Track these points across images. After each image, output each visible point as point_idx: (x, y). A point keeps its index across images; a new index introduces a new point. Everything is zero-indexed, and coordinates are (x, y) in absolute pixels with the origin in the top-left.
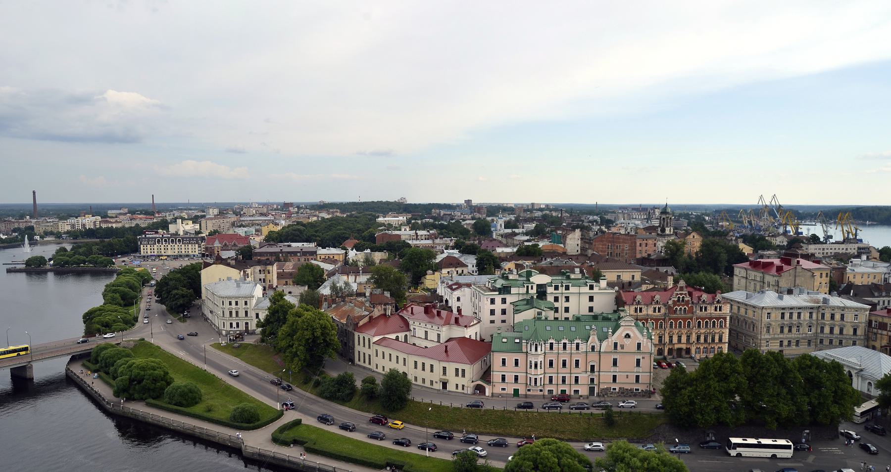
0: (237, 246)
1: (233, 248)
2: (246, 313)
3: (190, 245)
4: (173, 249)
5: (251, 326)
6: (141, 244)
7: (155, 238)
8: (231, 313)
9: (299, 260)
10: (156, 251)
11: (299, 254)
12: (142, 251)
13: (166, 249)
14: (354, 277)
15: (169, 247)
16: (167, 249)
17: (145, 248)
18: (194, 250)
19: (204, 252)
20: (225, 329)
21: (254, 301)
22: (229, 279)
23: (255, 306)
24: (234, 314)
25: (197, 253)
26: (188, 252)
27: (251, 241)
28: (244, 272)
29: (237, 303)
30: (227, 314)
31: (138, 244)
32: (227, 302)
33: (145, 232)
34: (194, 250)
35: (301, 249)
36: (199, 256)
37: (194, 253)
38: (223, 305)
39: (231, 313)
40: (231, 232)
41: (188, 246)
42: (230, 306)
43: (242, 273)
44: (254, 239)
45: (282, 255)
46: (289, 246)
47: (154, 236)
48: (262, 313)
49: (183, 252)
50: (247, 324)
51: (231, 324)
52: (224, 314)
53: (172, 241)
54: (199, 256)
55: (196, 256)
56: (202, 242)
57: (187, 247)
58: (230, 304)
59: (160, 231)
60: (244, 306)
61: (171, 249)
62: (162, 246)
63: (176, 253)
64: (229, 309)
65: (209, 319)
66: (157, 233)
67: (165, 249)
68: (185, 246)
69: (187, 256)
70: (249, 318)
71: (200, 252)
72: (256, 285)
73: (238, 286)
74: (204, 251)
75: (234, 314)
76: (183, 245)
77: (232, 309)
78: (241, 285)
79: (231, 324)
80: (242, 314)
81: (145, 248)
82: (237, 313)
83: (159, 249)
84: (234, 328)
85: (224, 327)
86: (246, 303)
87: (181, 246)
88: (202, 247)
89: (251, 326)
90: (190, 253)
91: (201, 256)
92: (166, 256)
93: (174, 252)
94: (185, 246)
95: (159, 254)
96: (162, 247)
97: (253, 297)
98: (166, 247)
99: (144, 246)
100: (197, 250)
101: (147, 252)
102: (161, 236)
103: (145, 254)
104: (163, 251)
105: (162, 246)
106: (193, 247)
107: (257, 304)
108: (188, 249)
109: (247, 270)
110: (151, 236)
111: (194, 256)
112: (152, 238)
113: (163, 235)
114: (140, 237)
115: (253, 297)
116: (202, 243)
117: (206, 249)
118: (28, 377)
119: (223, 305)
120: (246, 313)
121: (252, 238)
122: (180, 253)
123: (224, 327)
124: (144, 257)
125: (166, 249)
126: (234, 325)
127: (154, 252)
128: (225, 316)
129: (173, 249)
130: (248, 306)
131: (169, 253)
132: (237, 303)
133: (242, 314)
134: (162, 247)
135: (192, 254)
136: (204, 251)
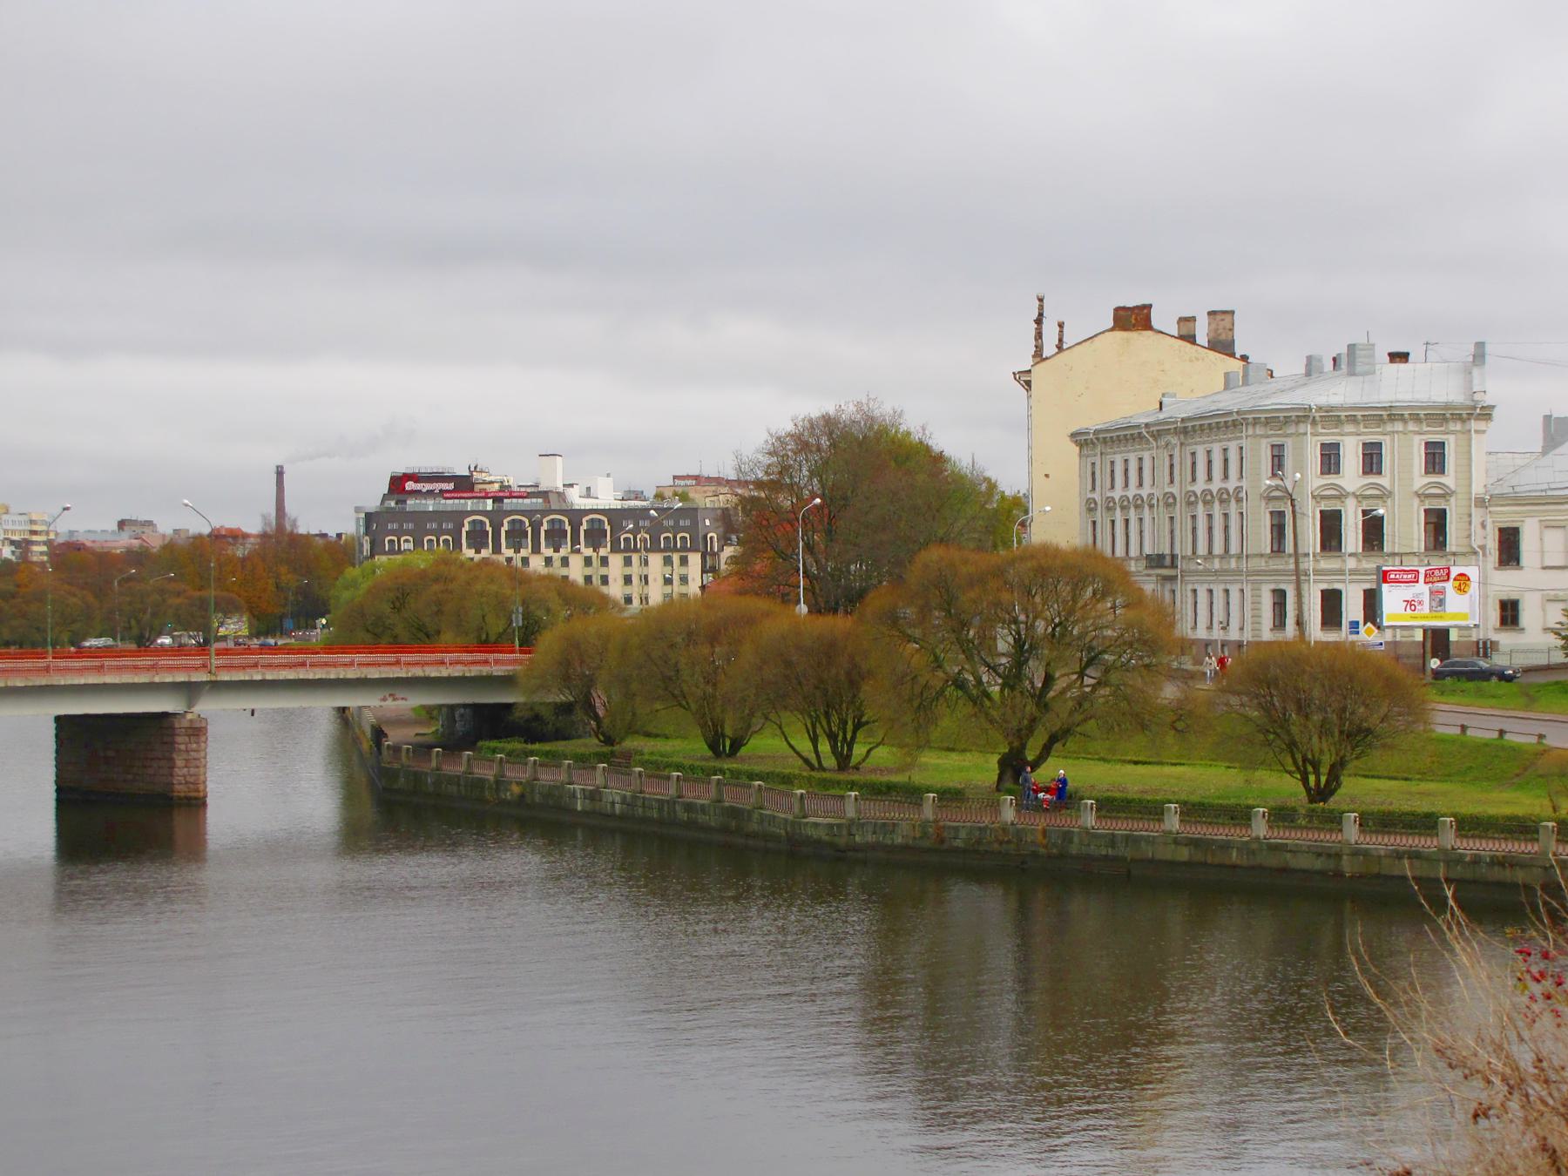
2: (1437, 524)
3: (656, 560)
8: (1331, 526)
24: (1352, 536)
29: (1372, 459)
39: (1331, 526)
51: (1332, 601)
57: (635, 570)
58: (1330, 459)
60: (1420, 480)
68: (628, 562)
75: (1352, 536)
76: (616, 561)
77: (1342, 496)
79: (1332, 601)
80: (1404, 530)
84: (1354, 625)
86: (1435, 458)
87: (604, 561)
94: (628, 562)
108: (645, 579)
110: (430, 505)
112: (438, 515)
118: (180, 789)
120: (1437, 524)
126: (1353, 608)
130: (1449, 480)
132: (1372, 459)
133: (1404, 530)
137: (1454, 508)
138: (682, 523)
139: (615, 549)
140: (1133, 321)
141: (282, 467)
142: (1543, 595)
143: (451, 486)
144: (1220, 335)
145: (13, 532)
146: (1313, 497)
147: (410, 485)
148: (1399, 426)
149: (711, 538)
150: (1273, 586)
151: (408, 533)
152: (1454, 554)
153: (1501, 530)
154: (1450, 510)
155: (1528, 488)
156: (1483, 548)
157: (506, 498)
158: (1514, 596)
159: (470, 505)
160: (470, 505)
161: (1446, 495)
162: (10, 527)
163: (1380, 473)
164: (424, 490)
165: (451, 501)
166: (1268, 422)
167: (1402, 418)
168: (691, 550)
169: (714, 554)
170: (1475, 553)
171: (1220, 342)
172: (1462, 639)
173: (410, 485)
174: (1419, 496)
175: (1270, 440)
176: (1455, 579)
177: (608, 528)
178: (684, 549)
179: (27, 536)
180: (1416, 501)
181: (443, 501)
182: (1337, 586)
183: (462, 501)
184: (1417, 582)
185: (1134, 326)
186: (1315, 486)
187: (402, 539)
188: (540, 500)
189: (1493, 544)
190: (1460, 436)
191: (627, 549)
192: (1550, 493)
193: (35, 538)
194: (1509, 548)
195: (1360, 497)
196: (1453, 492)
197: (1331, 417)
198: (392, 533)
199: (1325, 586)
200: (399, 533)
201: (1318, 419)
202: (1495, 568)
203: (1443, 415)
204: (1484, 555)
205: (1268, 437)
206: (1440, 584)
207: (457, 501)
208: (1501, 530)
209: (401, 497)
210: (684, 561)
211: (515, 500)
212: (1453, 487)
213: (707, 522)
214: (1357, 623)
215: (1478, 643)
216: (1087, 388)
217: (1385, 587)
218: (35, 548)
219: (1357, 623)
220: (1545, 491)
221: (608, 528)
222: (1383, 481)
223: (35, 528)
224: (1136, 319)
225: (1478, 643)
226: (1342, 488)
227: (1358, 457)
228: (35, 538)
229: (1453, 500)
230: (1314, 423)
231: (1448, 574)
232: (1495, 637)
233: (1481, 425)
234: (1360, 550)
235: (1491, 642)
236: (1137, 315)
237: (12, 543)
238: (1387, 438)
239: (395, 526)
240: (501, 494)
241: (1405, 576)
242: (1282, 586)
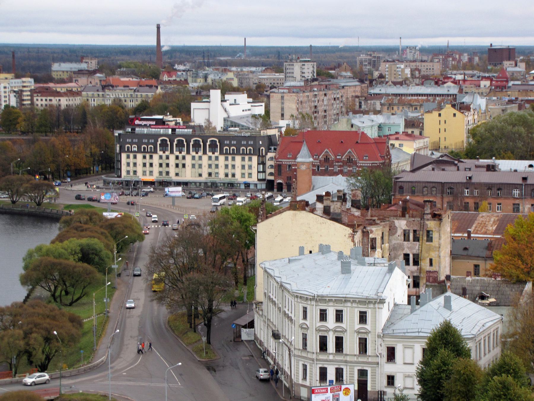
0: (355, 163)
1: (346, 169)
3: (238, 158)
4: (197, 166)
5: (374, 381)
6: (122, 150)
7: (156, 136)
9: (516, 209)
10: (156, 169)
11: (516, 192)
12: (124, 168)
13: (180, 166)
14: (247, 45)
15: (188, 160)
16: (184, 166)
17: (131, 160)
18: (246, 171)
19: (272, 178)
20: (307, 383)
21: (384, 314)
22: (324, 249)
23: (386, 327)
25: (254, 179)
26: (233, 175)
27: (392, 152)
28: (365, 234)
30: (314, 344)
31: (114, 149)
32: (314, 313)
33: (133, 120)
34: (246, 171)
35: (525, 179)
36: (259, 187)
37: (247, 180)
38: (305, 317)
40: (342, 126)
41: (233, 159)
42: (323, 323)
43: (358, 236)
44: (401, 145)
45: (472, 193)
46: (491, 168)
47: (153, 130)
48: (405, 347)
49: (222, 176)
50: (363, 373)
52: (305, 344)
53: (197, 146)
54: (259, 187)
55: (252, 187)
56: (268, 150)
58: (323, 316)
59: (169, 118)
60: (357, 326)
61: (193, 166)
62: (172, 157)
63: (205, 178)
64: (318, 330)
65: (269, 354)
66: (161, 123)
67: (177, 165)
68: (227, 159)
69: (231, 185)
70: (370, 360)
71: (261, 176)
72: (391, 270)
73: (346, 269)
74: (271, 174)
76: (222, 158)
77: (328, 330)
78: (352, 267)
81: (131, 160)
82: (339, 343)
83: (164, 165)
84: (331, 382)
85: (305, 378)
86: (363, 318)
87: (217, 158)
88: (269, 163)
89: (374, 381)
90: (239, 178)
91: (264, 186)
92: (178, 184)
93: (200, 175)
95: (164, 178)
96: (172, 160)
97: (382, 301)
98: (180, 162)
99: (128, 157)
100: (254, 171)
101: (135, 172)
102: (170, 130)
103: (131, 177)
104: (172, 170)
105: (172, 157)
106: (247, 163)
107: (390, 322)
108: (233, 166)
109: (374, 228)
110: (145, 131)
111: (247, 185)
113: (174, 130)
114: (121, 132)
115: (382, 301)
116: (270, 155)
117: (279, 168)
119: (305, 317)
121: (397, 143)
122: (213, 179)
123: (305, 378)
124: (128, 183)
125: (180, 166)
127: (151, 173)
128: (309, 348)
129: (197, 166)
131: (188, 175)
134: (172, 160)
135: (243, 180)
136: (271, 174)
137: (370, 337)
138: (250, 143)
139: (221, 153)
140: (298, 207)
141: (159, 25)
142: (404, 374)
143: (154, 123)
144: (335, 210)
145: (15, 87)
146: (316, 330)
147: (137, 122)
148: (349, 304)
149: (262, 150)
150: (303, 363)
151: (135, 143)
152: (369, 356)
153: (388, 348)
154: (369, 339)
155: (399, 331)
156: (381, 354)
157: (177, 128)
158: (392, 374)
159: (162, 131)
160: (162, 131)
161: (367, 333)
162: (14, 85)
163: (342, 322)
164: (143, 124)
165: (154, 130)
166: (301, 297)
167: (349, 301)
168: (254, 154)
169: (263, 156)
170: (378, 356)
171: (335, 213)
172: (373, 390)
173: (137, 122)
174: (357, 332)
175: (302, 304)
176: (344, 390)
177: (218, 144)
178: (250, 154)
179: (21, 88)
180: (356, 334)
181: (151, 129)
182: (325, 366)
183: (159, 130)
184: (327, 392)
185: (298, 209)
186: (317, 326)
187: (133, 146)
188: (191, 130)
189: (385, 353)
190: (372, 309)
191: (226, 153)
192: (407, 334)
193: (25, 89)
194: (391, 354)
195: (335, 331)
196: (370, 332)
197: (320, 299)
198: (129, 143)
199: (321, 366)
200: (131, 143)
201: (318, 300)
202: (386, 363)
203: (366, 301)
204: (381, 357)
205: (302, 303)
206: (337, 393)
207: (156, 130)
208: (388, 348)
209: (133, 127)
210: (250, 159)
211: (181, 130)
212: (370, 330)
213: (261, 143)
214: (333, 381)
215: (378, 392)
216: (279, 233)
217: (313, 395)
218: (25, 93)
219: (333, 381)
220: (405, 333)
221: (218, 144)
222: (343, 325)
223: (25, 84)
224: (299, 206)
225: (378, 392)
226: (327, 327)
227: (334, 315)
228: (25, 89)
229: (370, 335)
230: (316, 301)
231: (341, 389)
232: (385, 390)
233: (381, 306)
234: (334, 352)
235: (383, 392)
236: (299, 204)
237: (14, 92)
238: (345, 309)
239: (130, 140)
240: (175, 127)
241: (322, 391)
242: (306, 364)
